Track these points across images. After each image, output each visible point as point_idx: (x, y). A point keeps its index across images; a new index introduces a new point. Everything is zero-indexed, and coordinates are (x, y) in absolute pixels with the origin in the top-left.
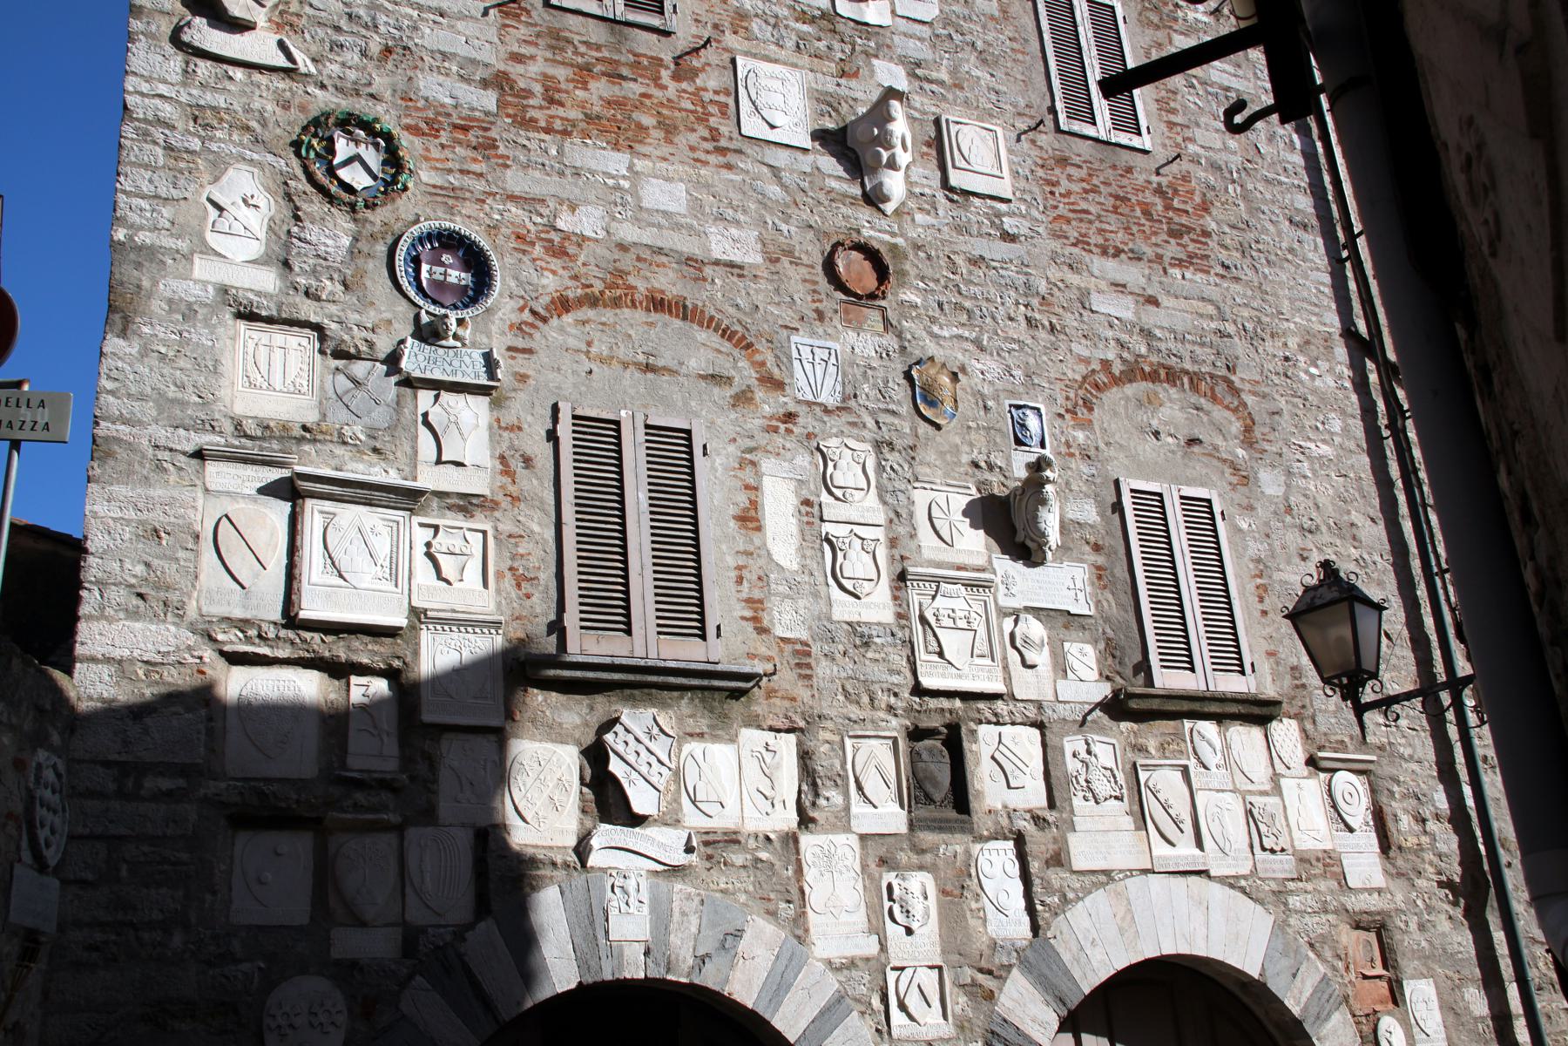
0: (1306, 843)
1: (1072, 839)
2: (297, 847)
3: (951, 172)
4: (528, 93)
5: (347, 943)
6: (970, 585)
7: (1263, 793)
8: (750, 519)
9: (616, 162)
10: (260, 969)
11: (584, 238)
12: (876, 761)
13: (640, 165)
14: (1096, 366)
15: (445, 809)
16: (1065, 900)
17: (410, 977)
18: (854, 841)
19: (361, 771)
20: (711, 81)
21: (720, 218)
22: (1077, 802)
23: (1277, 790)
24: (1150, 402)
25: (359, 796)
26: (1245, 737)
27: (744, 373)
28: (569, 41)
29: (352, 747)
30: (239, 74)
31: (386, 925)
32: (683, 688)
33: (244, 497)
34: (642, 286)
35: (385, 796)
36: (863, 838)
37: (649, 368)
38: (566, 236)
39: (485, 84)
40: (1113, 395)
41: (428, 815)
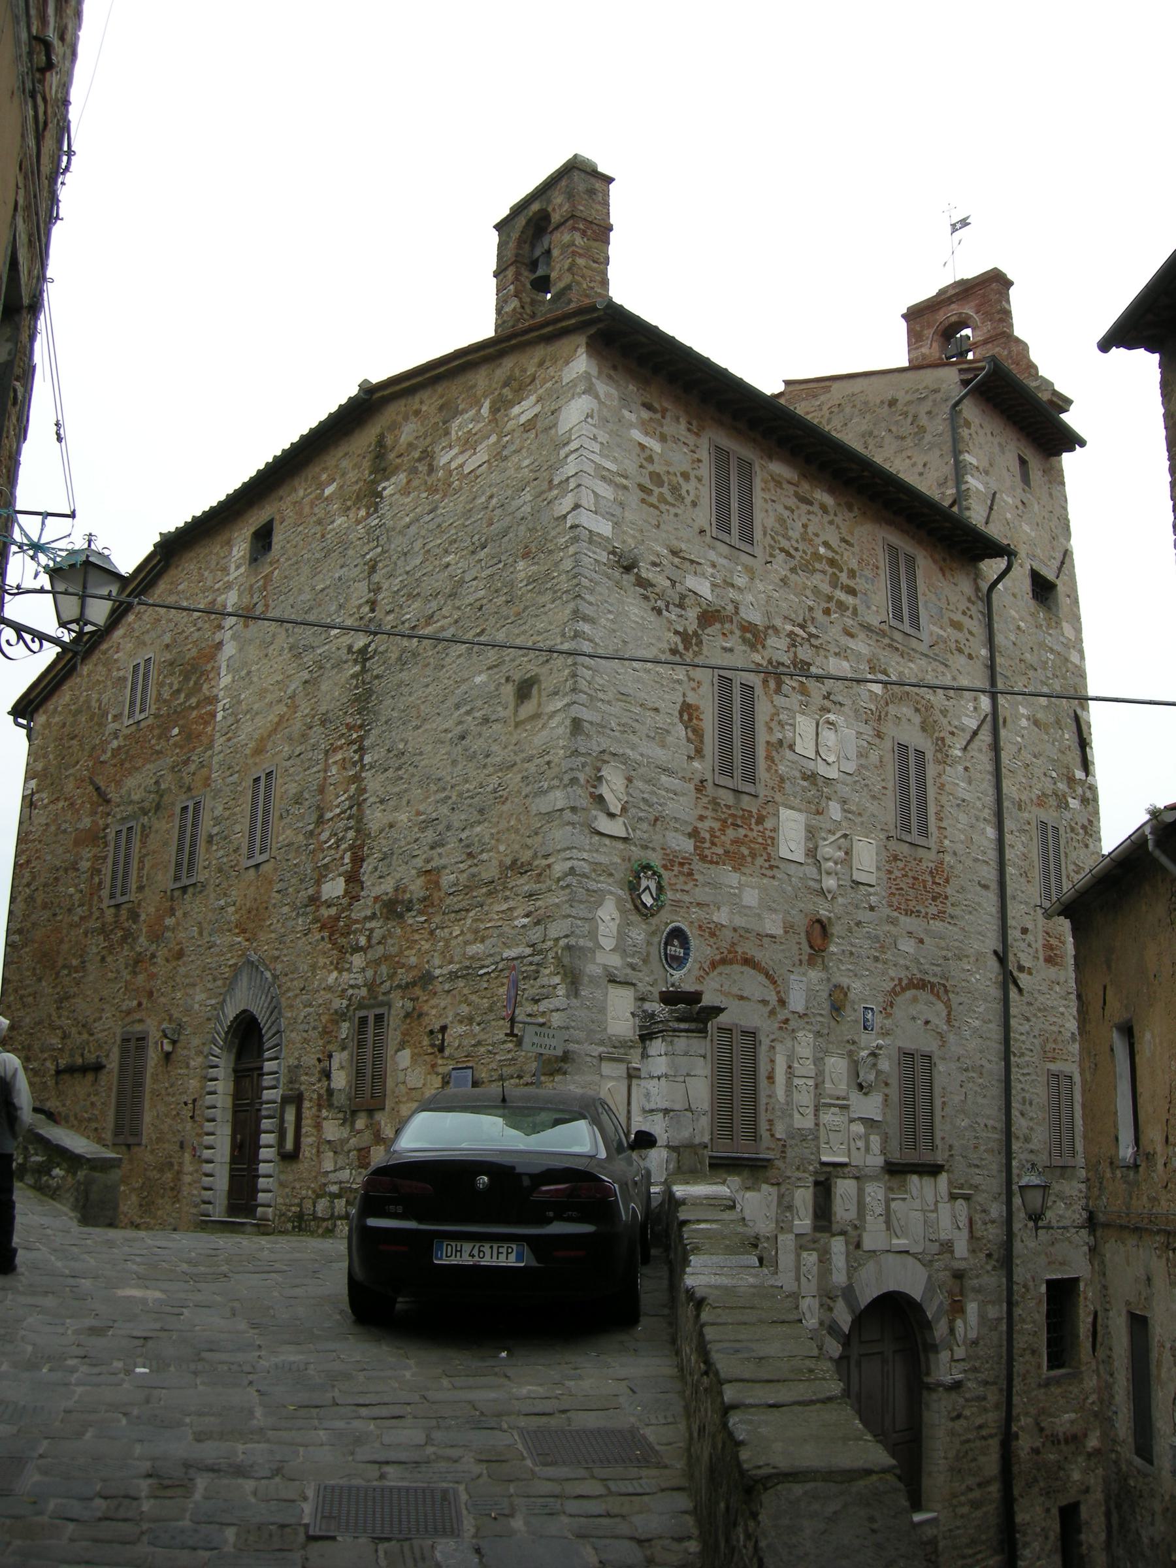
0: (944, 1236)
1: (865, 1235)
3: (855, 872)
4: (703, 841)
6: (842, 1107)
7: (932, 1211)
8: (771, 1078)
9: (733, 878)
11: (723, 926)
12: (804, 1197)
13: (743, 878)
14: (896, 982)
16: (860, 1265)
18: (791, 1236)
20: (769, 824)
21: (770, 909)
22: (868, 1218)
23: (936, 1210)
24: (915, 1000)
26: (927, 1181)
27: (773, 998)
28: (719, 804)
30: (607, 841)
32: (747, 1166)
33: (613, 1078)
34: (740, 950)
36: (797, 1235)
37: (742, 998)
38: (717, 925)
39: (690, 835)
40: (899, 1000)
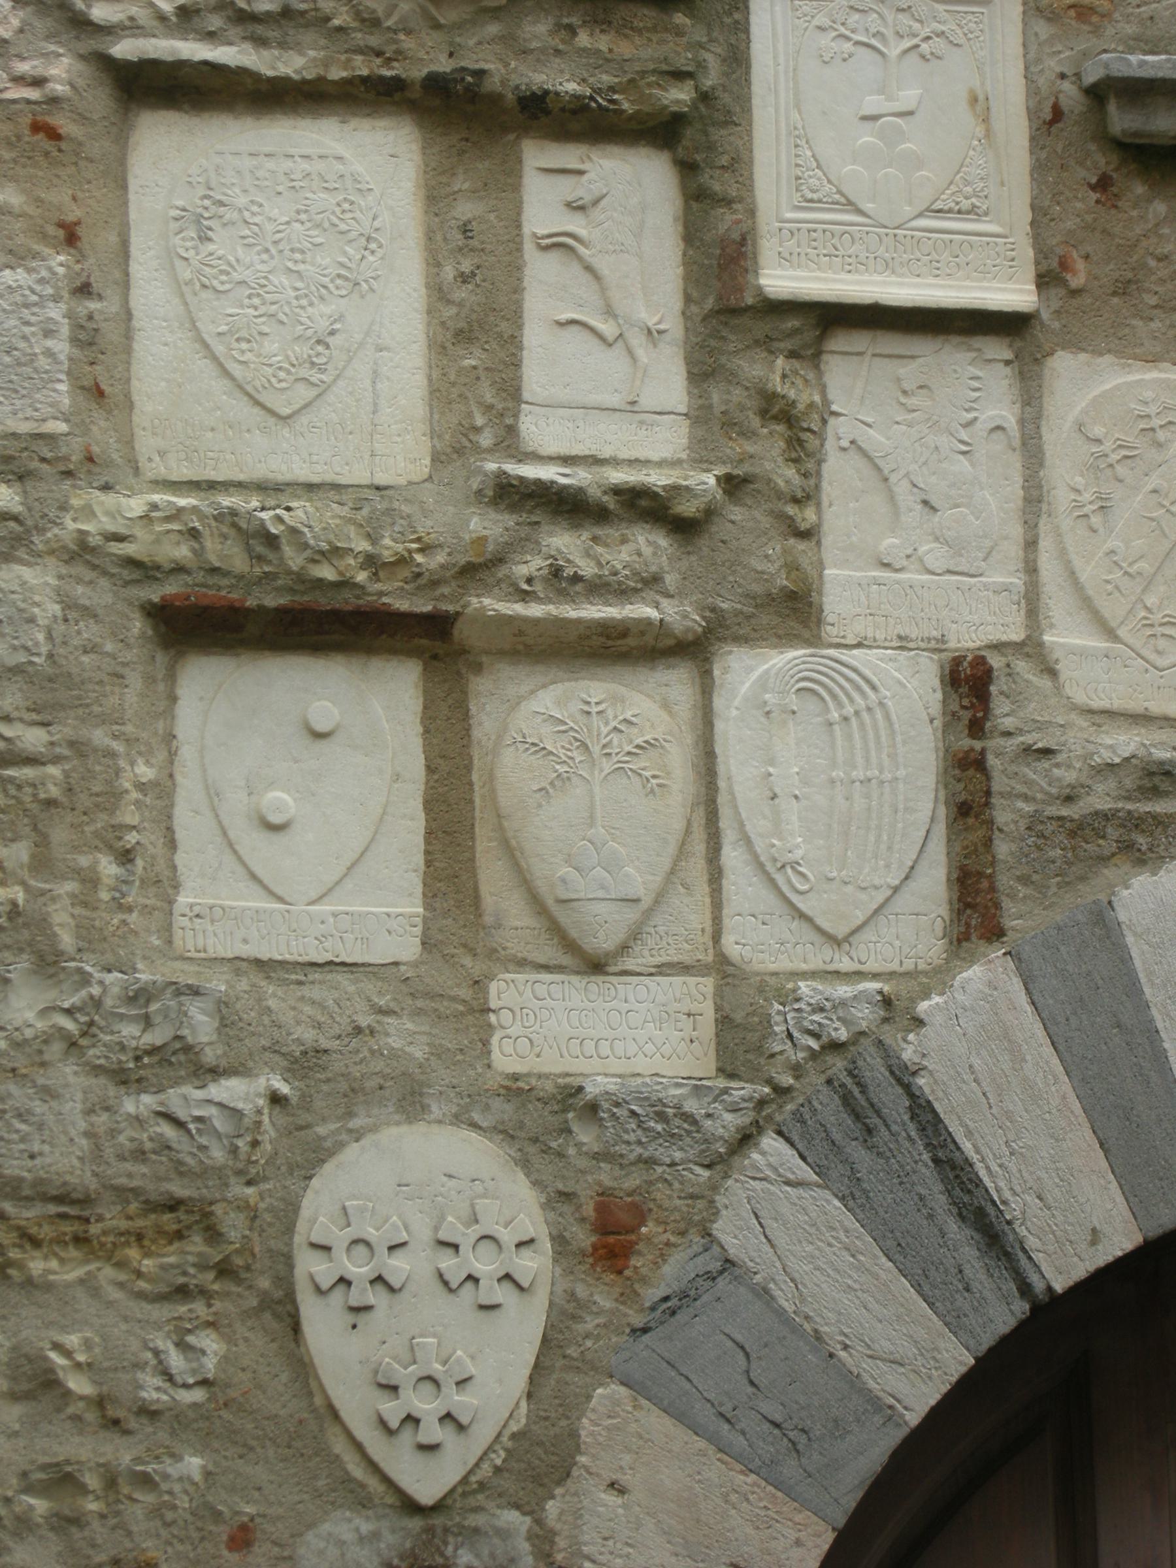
2: (374, 707)
5: (550, 1028)
10: (276, 1099)
15: (843, 588)
17: (746, 1139)
19: (567, 460)
25: (565, 543)
29: (535, 379)
31: (662, 970)
35: (646, 545)
41: (794, 611)
